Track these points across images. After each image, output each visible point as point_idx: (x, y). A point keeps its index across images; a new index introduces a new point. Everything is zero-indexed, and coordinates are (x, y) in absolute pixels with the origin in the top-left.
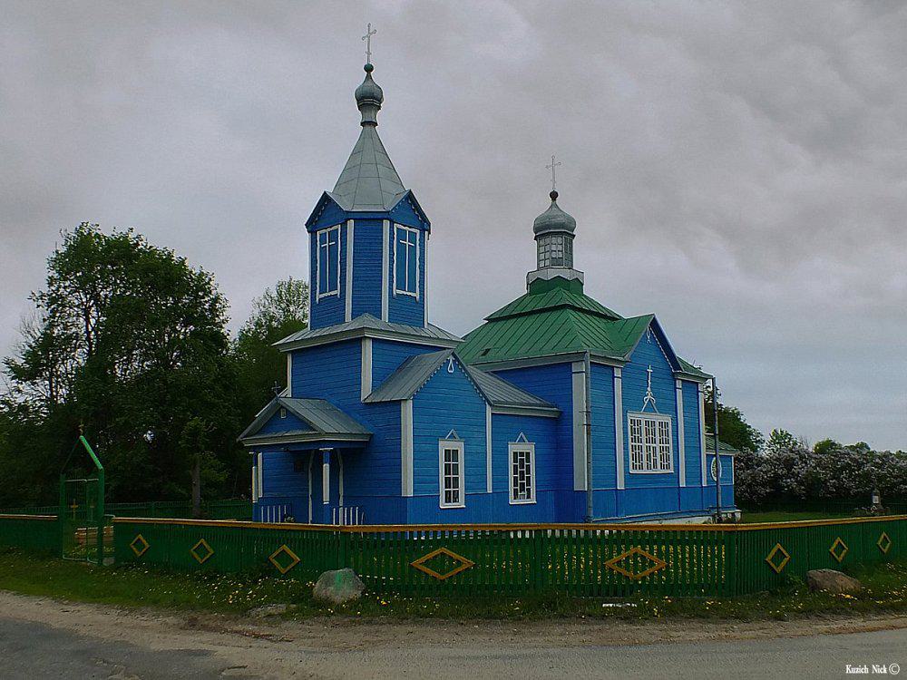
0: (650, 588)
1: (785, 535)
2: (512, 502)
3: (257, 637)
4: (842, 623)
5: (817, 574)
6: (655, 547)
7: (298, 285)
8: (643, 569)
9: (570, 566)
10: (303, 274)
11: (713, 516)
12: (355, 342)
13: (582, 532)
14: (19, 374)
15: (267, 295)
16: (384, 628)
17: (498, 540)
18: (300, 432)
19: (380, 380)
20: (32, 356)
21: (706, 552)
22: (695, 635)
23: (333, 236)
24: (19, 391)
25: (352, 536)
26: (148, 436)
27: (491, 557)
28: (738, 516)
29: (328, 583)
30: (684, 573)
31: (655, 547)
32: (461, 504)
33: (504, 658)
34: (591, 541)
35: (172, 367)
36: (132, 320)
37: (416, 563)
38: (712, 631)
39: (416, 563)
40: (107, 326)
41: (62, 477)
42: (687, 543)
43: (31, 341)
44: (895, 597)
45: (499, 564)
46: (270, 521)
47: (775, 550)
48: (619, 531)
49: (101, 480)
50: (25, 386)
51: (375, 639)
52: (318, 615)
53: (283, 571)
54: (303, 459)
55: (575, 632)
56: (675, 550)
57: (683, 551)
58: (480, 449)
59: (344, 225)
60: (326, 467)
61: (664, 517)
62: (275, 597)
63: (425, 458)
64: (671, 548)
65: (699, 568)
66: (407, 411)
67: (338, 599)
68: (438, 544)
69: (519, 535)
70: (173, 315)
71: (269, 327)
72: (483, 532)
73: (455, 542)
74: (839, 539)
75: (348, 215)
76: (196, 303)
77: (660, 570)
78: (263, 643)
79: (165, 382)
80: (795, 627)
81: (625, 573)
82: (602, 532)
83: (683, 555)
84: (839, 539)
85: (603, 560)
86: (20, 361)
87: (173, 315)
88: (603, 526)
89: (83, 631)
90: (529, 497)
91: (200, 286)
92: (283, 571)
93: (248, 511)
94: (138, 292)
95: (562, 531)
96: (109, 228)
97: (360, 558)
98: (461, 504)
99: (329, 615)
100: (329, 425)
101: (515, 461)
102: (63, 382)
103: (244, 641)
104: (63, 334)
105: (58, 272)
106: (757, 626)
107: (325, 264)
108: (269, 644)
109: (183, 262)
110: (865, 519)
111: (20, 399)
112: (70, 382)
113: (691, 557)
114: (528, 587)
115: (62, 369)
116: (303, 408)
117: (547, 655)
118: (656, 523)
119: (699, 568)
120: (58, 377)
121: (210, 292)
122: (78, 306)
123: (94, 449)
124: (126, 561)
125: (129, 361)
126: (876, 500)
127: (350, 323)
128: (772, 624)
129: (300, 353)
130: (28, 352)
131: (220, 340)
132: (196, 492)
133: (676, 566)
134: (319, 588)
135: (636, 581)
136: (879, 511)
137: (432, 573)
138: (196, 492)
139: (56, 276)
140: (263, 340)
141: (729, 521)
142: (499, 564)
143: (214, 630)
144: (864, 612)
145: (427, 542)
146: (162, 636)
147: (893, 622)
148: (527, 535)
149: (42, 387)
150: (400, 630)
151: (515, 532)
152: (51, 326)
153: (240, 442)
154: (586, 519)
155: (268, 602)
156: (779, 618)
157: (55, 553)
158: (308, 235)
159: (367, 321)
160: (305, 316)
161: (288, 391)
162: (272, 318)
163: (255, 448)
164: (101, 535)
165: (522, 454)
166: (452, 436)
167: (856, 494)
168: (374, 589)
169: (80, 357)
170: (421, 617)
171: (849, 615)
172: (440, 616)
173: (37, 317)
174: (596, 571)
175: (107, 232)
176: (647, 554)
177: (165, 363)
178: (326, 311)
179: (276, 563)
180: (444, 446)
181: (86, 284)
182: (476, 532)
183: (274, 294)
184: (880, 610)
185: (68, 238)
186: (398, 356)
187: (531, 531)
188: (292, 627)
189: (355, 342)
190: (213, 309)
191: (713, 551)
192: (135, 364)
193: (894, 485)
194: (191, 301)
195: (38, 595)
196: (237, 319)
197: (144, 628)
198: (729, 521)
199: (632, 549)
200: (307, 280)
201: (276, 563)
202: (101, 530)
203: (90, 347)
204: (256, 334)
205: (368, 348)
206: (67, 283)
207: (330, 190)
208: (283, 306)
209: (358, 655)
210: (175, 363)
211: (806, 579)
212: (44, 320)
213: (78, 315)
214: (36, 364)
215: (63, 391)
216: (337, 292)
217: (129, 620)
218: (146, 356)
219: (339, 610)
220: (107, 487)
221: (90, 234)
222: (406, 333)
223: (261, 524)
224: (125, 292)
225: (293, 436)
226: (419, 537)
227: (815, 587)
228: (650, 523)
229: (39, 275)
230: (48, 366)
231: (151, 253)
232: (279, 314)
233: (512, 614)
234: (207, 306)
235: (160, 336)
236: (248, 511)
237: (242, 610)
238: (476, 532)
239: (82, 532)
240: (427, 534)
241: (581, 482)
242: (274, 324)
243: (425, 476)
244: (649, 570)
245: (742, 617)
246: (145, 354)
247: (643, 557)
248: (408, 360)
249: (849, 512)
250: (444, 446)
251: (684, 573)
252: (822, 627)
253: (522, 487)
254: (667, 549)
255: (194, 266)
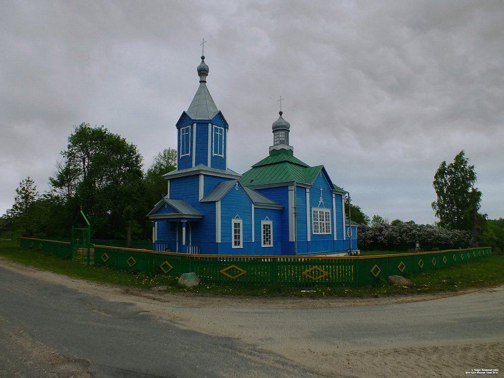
0: (320, 284)
1: (380, 261)
2: (263, 246)
3: (154, 299)
4: (404, 298)
5: (392, 278)
6: (324, 266)
7: (173, 151)
8: (319, 276)
9: (287, 274)
10: (174, 146)
11: (348, 253)
12: (196, 176)
13: (293, 259)
14: (55, 184)
15: (160, 155)
16: (207, 298)
17: (257, 262)
18: (173, 214)
19: (207, 193)
20: (61, 177)
21: (345, 269)
22: (341, 304)
23: (187, 130)
24: (55, 191)
25: (195, 259)
26: (109, 212)
27: (254, 270)
28: (359, 253)
29: (185, 278)
30: (336, 277)
31: (324, 266)
32: (241, 246)
33: (259, 313)
34: (296, 264)
35: (119, 184)
36: (103, 164)
37: (222, 271)
38: (349, 302)
39: (222, 271)
40: (92, 166)
41: (73, 227)
42: (337, 264)
43: (61, 170)
44: (425, 287)
45: (257, 272)
46: (160, 250)
47: (374, 267)
48: (308, 259)
49: (88, 229)
50: (58, 189)
51: (205, 303)
52: (181, 292)
53: (166, 272)
54: (174, 225)
55: (289, 303)
56: (332, 267)
57: (335, 268)
58: (249, 223)
59: (192, 125)
60: (184, 229)
61: (327, 253)
62: (162, 283)
63: (226, 226)
64: (330, 267)
65: (342, 275)
66: (218, 206)
67: (189, 285)
68: (231, 263)
69: (266, 260)
70: (119, 163)
71: (160, 169)
72: (251, 259)
73: (239, 263)
74: (402, 263)
75: (194, 121)
76: (130, 157)
77: (325, 276)
78: (156, 302)
79: (116, 190)
80: (384, 301)
81: (310, 277)
82: (301, 260)
83: (335, 269)
84: (402, 263)
85: (301, 272)
86: (56, 179)
87: (119, 163)
88: (302, 257)
89: (80, 291)
90: (270, 244)
91: (131, 150)
92: (166, 272)
93: (152, 246)
94: (105, 152)
95: (284, 259)
96: (94, 125)
97: (198, 268)
98: (241, 246)
99: (185, 292)
100: (185, 211)
101: (264, 228)
102: (74, 188)
103: (149, 301)
104: (74, 168)
105: (72, 143)
106: (366, 300)
107: (184, 142)
108: (159, 302)
109: (124, 140)
110: (413, 254)
111: (56, 194)
112: (77, 189)
113: (339, 271)
114: (269, 283)
115: (73, 183)
116: (171, 202)
117: (277, 313)
118: (324, 256)
119: (342, 275)
120: (72, 186)
121: (136, 153)
122: (80, 157)
123: (87, 217)
124: (99, 264)
125: (101, 181)
126: (417, 245)
127: (194, 168)
128: (373, 299)
129: (173, 180)
130: (59, 175)
131: (139, 173)
132: (129, 237)
133: (332, 275)
134: (181, 280)
135: (315, 281)
136: (419, 250)
137: (229, 276)
138: (129, 237)
139: (71, 144)
140: (158, 173)
141: (355, 255)
142: (257, 272)
143: (137, 295)
144: (412, 294)
145: (226, 263)
146: (114, 295)
147: (425, 298)
148: (269, 261)
149: (65, 190)
150: (215, 300)
151: (264, 259)
152: (69, 165)
153: (148, 217)
154: (294, 254)
155: (159, 285)
156: (376, 297)
157: (69, 258)
158: (177, 130)
159: (201, 167)
160: (175, 164)
161: (168, 196)
162: (162, 165)
163: (153, 220)
164: (89, 252)
165: (267, 225)
166: (237, 217)
167: (409, 243)
168: (204, 282)
169: (81, 178)
170: (224, 294)
171: (406, 295)
172: (232, 294)
173: (63, 161)
174: (299, 278)
175: (93, 127)
176: (320, 269)
177: (116, 182)
178: (184, 162)
179: (162, 268)
180: (234, 221)
181: (84, 148)
182: (247, 259)
183: (163, 155)
184: (419, 293)
185: (76, 129)
186: (215, 182)
187: (271, 259)
188: (169, 296)
189: (196, 176)
190: (137, 161)
191: (348, 268)
192: (104, 182)
193: (425, 239)
194: (127, 157)
195: (62, 274)
196: (147, 165)
197: (106, 292)
198: (355, 255)
199: (314, 267)
200: (176, 149)
201: (162, 268)
202: (89, 250)
203: (85, 174)
204: (155, 171)
205: (202, 178)
206: (76, 148)
207: (186, 110)
208: (166, 160)
209: (197, 309)
210: (120, 182)
211: (387, 279)
212: (66, 163)
213: (80, 161)
214: (63, 179)
215: (74, 192)
216: (189, 154)
217: (100, 288)
218: (108, 179)
219: (189, 290)
220: (91, 233)
221: (85, 127)
222: (218, 172)
223: (156, 252)
224: (100, 152)
225: (170, 215)
226: (223, 260)
227: (391, 283)
228: (321, 256)
229: (64, 144)
230: (67, 182)
231: (111, 136)
232: (164, 163)
233: (263, 294)
234: (134, 159)
235: (115, 171)
236: (152, 246)
237: (148, 288)
238: (247, 259)
239: (81, 250)
240: (227, 259)
241: (292, 238)
242: (163, 167)
243: (226, 234)
244: (321, 276)
245: (361, 297)
246: (108, 178)
247: (318, 270)
248: (219, 184)
249: (406, 251)
250: (234, 221)
251: (336, 277)
252: (394, 300)
253: (267, 240)
254: (329, 267)
255: (129, 142)
